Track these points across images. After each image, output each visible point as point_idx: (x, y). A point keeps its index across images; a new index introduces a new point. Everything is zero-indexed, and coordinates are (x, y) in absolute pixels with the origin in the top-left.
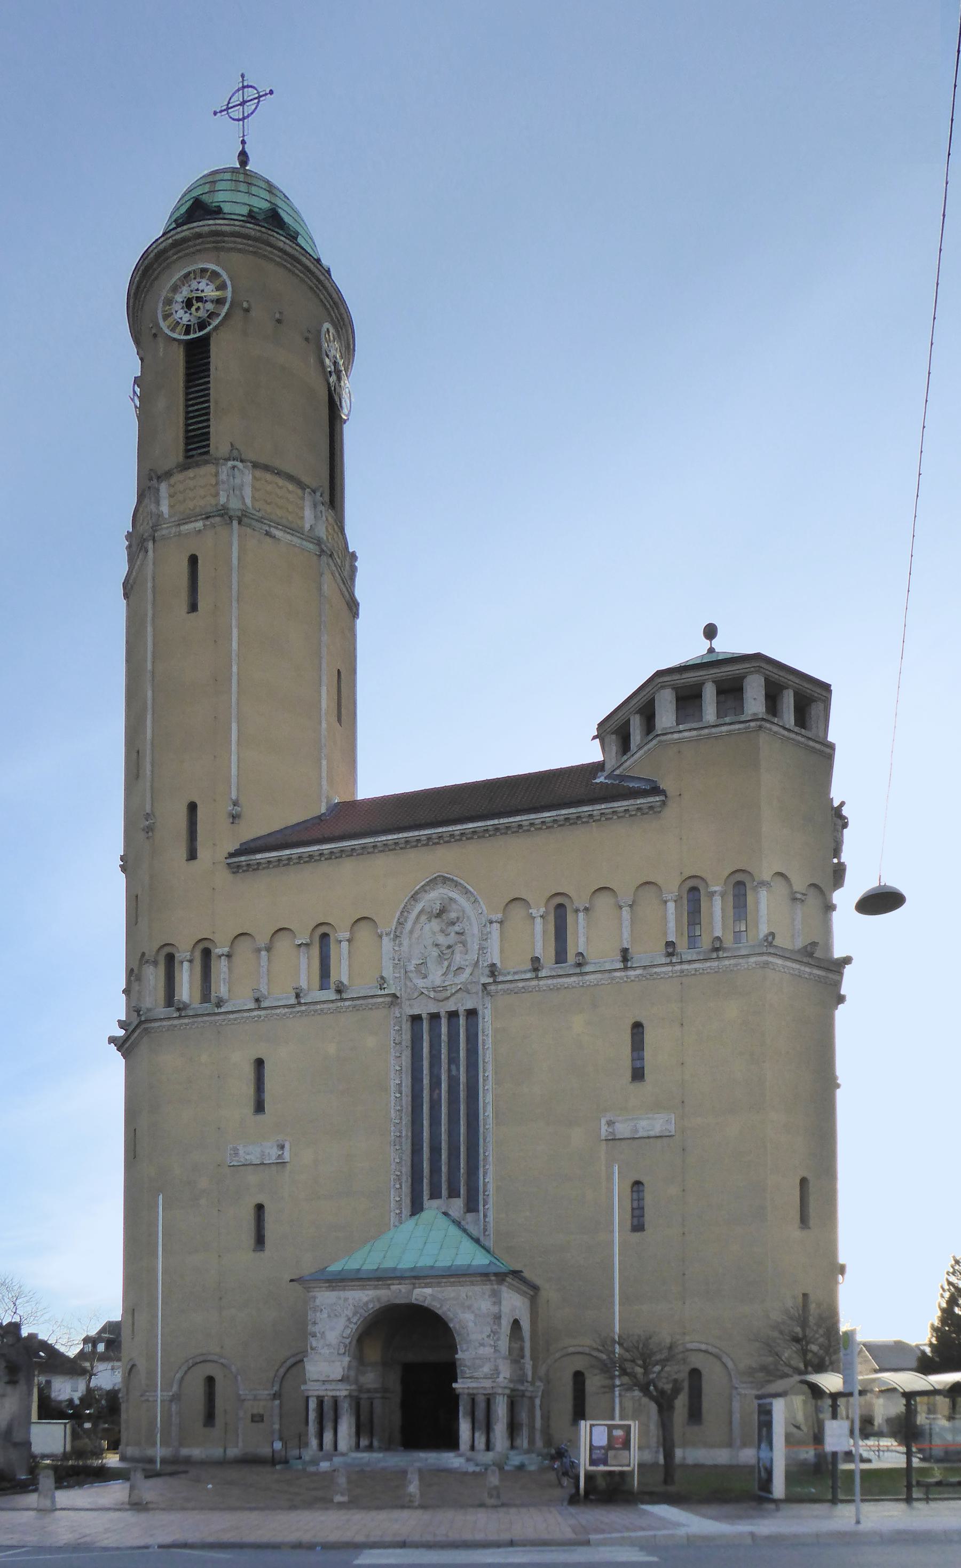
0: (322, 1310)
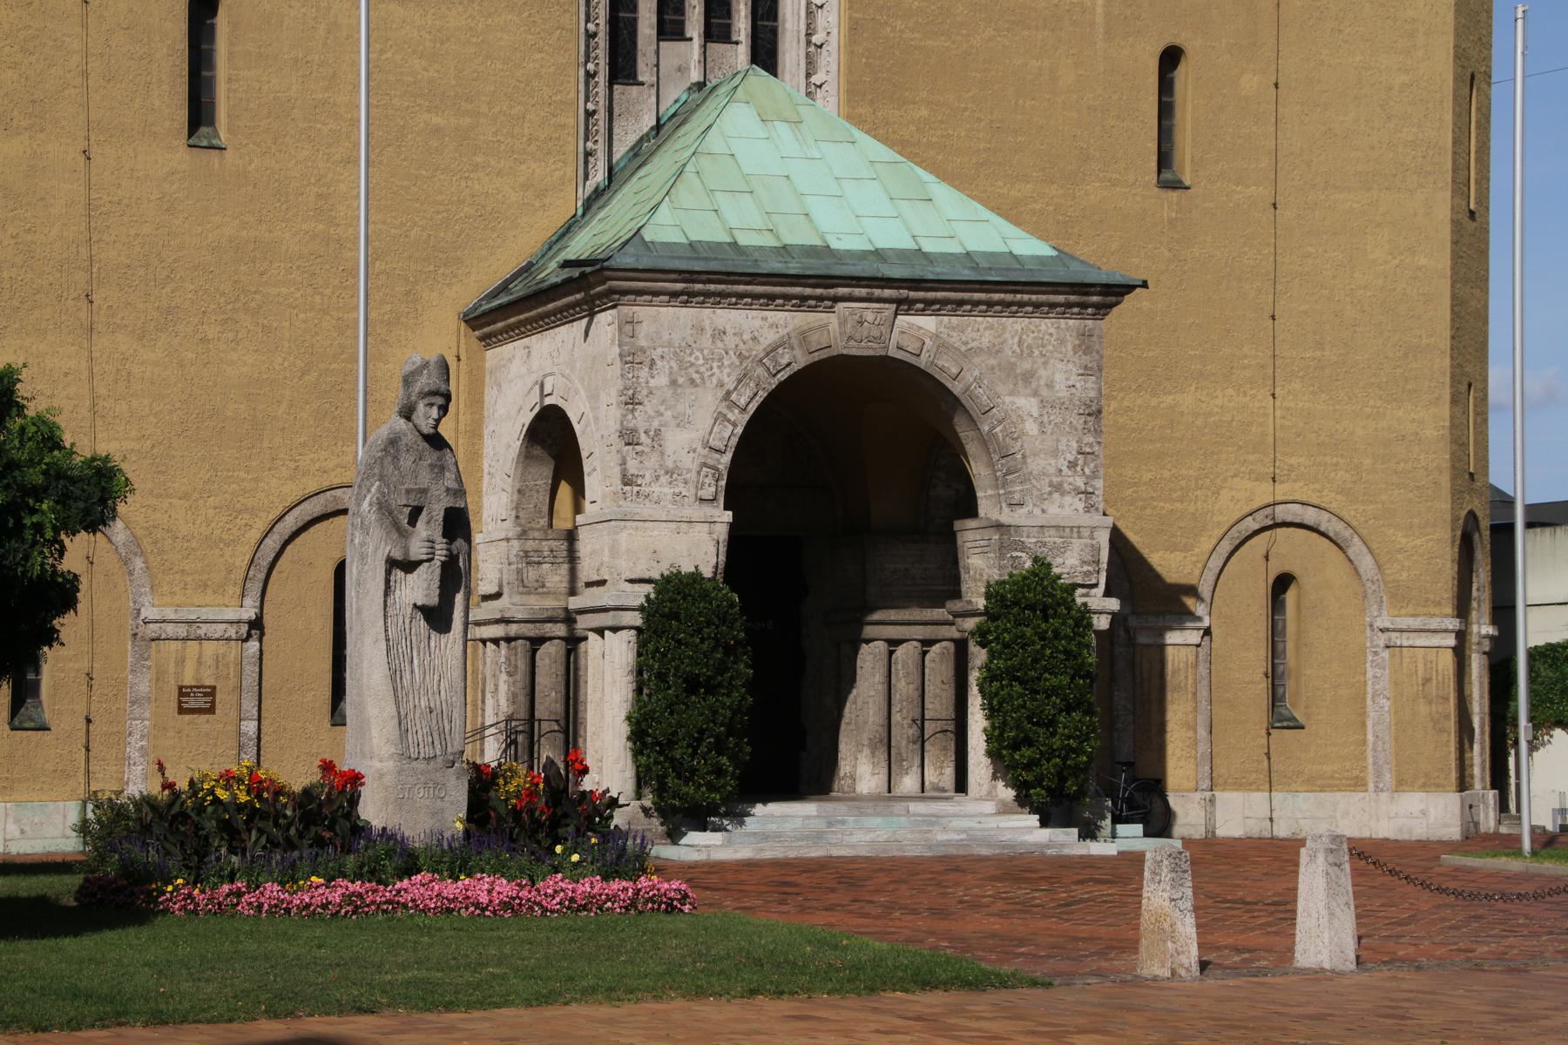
0: (653, 363)
